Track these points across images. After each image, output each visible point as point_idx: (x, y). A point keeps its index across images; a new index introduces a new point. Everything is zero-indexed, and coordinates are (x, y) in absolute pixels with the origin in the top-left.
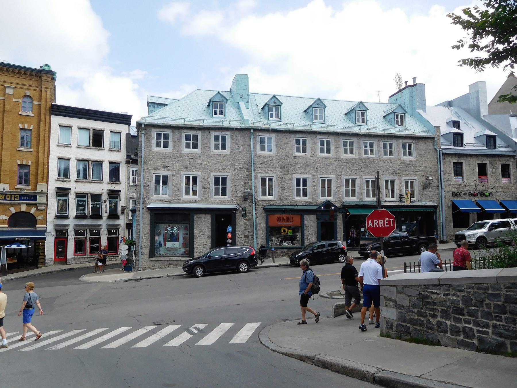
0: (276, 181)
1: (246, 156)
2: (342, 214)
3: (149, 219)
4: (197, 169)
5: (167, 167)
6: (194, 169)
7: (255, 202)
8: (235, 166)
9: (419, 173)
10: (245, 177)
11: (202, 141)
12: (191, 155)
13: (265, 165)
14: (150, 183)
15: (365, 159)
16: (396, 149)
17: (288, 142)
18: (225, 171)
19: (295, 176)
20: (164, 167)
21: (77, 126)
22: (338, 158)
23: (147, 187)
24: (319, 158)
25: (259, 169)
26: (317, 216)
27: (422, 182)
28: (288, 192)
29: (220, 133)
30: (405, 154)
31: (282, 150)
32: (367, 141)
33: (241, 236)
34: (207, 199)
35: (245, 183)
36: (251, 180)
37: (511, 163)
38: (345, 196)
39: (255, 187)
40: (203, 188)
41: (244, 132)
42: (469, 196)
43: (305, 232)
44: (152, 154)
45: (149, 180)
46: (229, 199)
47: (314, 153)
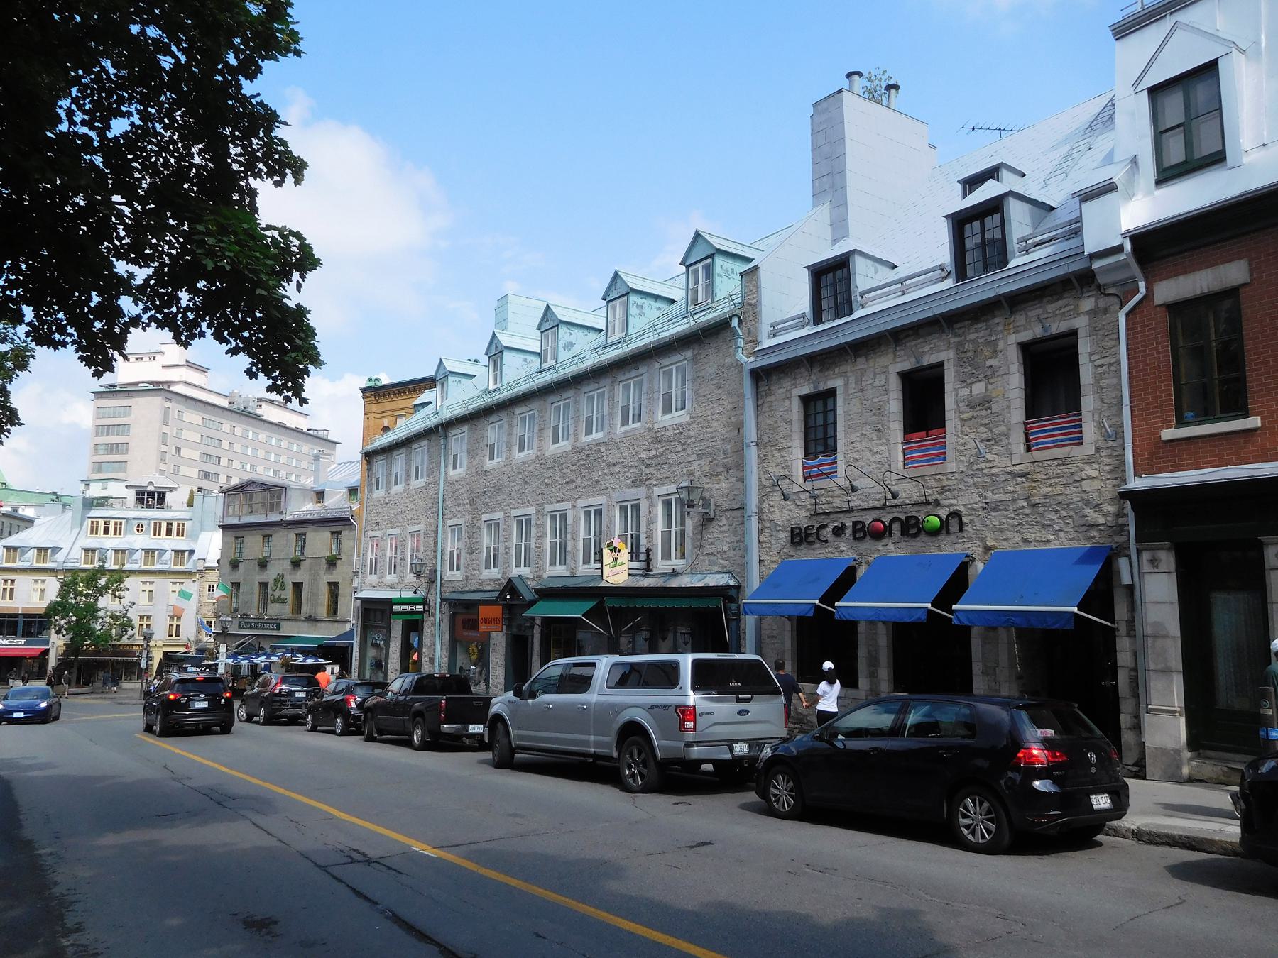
37: (1081, 323)
38: (548, 564)
42: (855, 538)
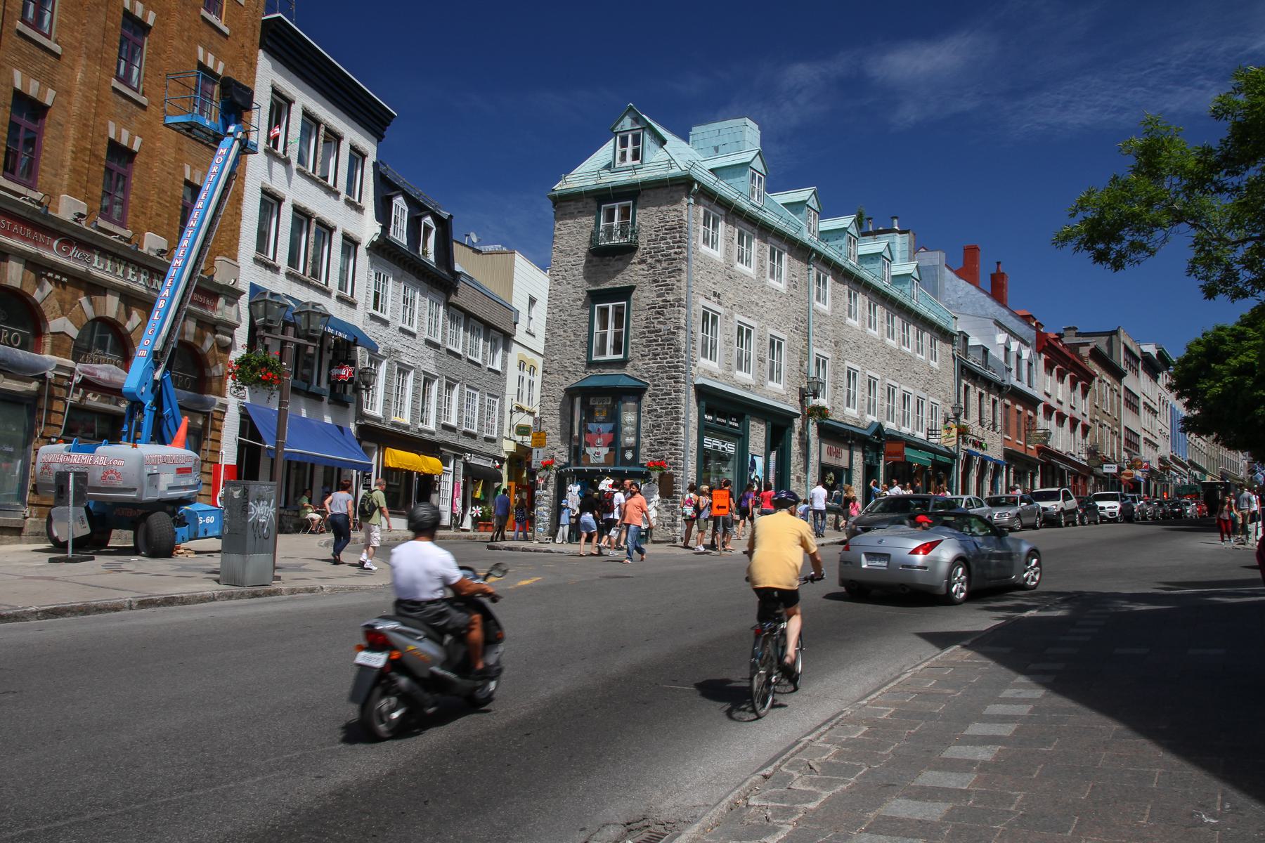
4: (752, 312)
20: (715, 294)
25: (816, 338)
34: (761, 385)
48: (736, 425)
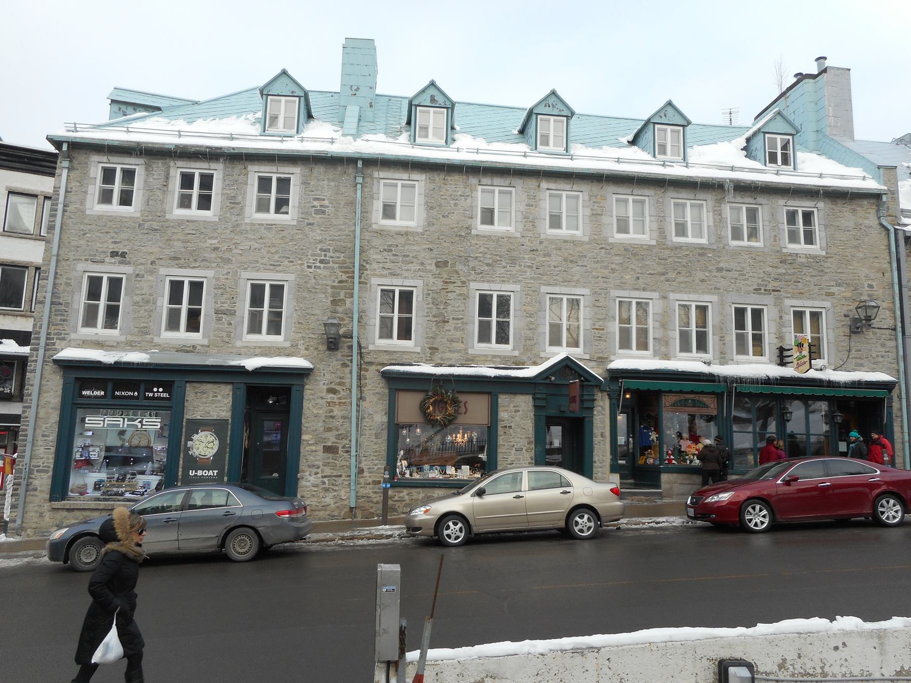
0: (420, 298)
1: (340, 230)
2: (609, 395)
3: (60, 392)
4: (203, 260)
5: (123, 255)
6: (195, 260)
7: (360, 354)
8: (309, 257)
9: (834, 289)
10: (334, 286)
11: (223, 189)
12: (191, 224)
13: (394, 255)
14: (72, 297)
15: (678, 248)
16: (767, 223)
17: (461, 196)
18: (280, 268)
19: (476, 288)
20: (114, 254)
21: (7, 188)
22: (599, 242)
23: (62, 307)
24: (546, 239)
25: (375, 266)
26: (534, 399)
27: (845, 316)
28: (455, 328)
29: (274, 169)
30: (793, 238)
31: (443, 216)
32: (684, 201)
33: (314, 448)
35: (334, 302)
36: (352, 296)
39: (362, 312)
40: (217, 312)
41: (339, 168)
43: (500, 441)
44: (86, 221)
45: (69, 289)
46: (288, 344)
47: (531, 227)
48: (165, 395)
